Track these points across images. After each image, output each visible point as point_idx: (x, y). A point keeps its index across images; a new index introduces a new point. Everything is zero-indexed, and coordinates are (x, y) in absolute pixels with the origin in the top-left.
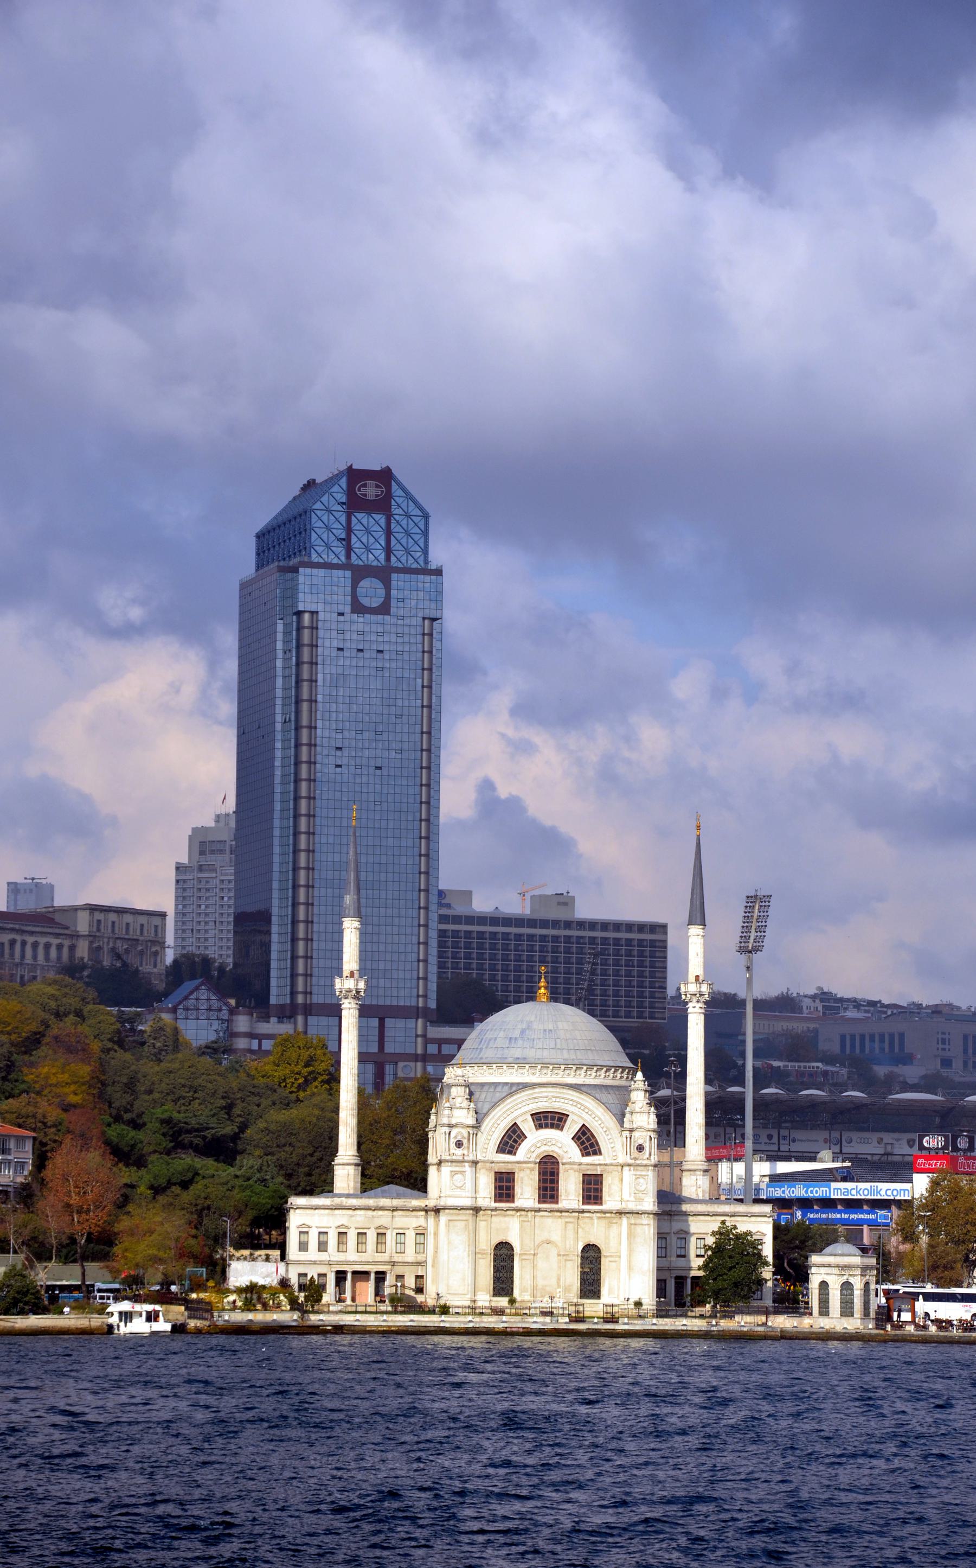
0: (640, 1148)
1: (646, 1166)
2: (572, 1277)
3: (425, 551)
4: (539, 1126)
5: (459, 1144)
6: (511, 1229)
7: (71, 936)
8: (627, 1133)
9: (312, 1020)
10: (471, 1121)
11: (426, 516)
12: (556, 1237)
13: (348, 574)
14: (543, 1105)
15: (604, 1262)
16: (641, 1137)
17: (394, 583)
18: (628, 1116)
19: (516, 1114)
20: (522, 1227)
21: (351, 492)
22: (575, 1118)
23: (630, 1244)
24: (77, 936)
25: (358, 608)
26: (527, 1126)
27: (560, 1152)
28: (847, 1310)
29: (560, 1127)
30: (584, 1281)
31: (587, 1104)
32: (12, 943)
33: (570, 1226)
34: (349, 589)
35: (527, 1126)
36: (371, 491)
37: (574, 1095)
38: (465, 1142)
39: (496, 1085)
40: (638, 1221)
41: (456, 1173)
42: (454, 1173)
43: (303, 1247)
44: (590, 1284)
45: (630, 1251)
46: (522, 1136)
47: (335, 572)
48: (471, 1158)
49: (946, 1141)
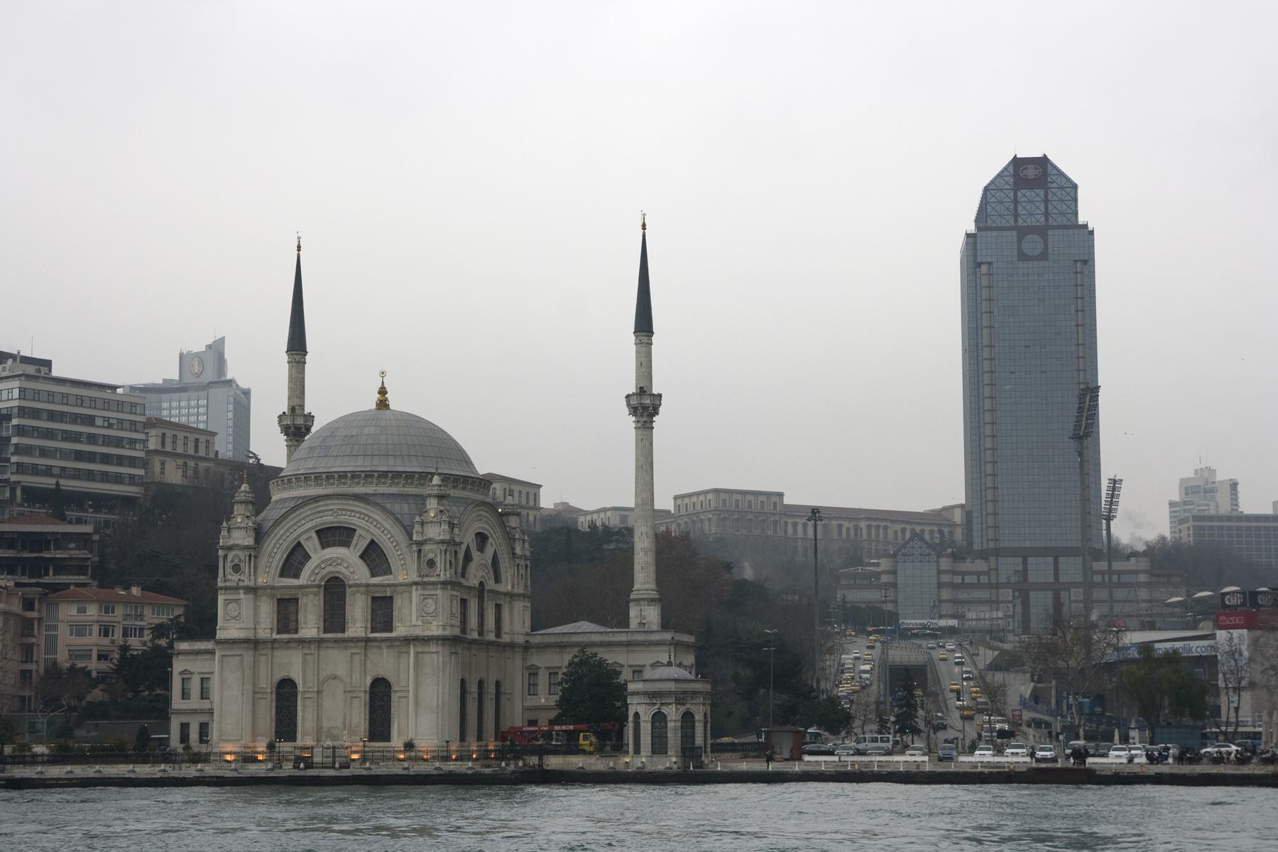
0: (431, 563)
1: (434, 583)
2: (359, 717)
3: (1076, 213)
4: (324, 545)
5: (236, 568)
6: (293, 665)
7: (949, 525)
8: (414, 548)
9: (1000, 559)
10: (250, 541)
11: (1075, 187)
12: (342, 671)
13: (1015, 233)
14: (328, 519)
15: (394, 697)
16: (431, 551)
17: (1050, 239)
18: (417, 527)
19: (299, 531)
20: (304, 661)
21: (1016, 175)
22: (363, 533)
23: (417, 676)
24: (955, 525)
25: (1022, 257)
26: (312, 545)
27: (346, 572)
28: (659, 747)
29: (346, 544)
30: (373, 722)
31: (376, 517)
32: (904, 530)
33: (357, 658)
34: (1015, 246)
35: (312, 545)
36: (1031, 172)
37: (360, 507)
38: (242, 565)
39: (285, 500)
40: (426, 649)
41: (230, 601)
42: (228, 602)
43: (185, 695)
44: (379, 726)
45: (417, 684)
46: (307, 557)
47: (1005, 233)
48: (246, 583)
49: (1245, 598)
